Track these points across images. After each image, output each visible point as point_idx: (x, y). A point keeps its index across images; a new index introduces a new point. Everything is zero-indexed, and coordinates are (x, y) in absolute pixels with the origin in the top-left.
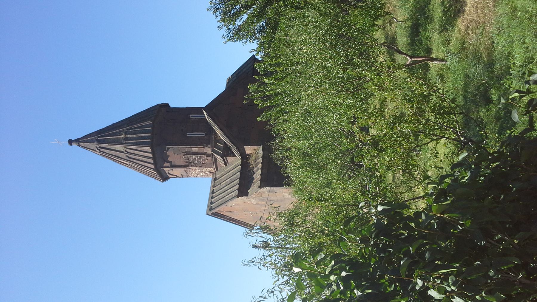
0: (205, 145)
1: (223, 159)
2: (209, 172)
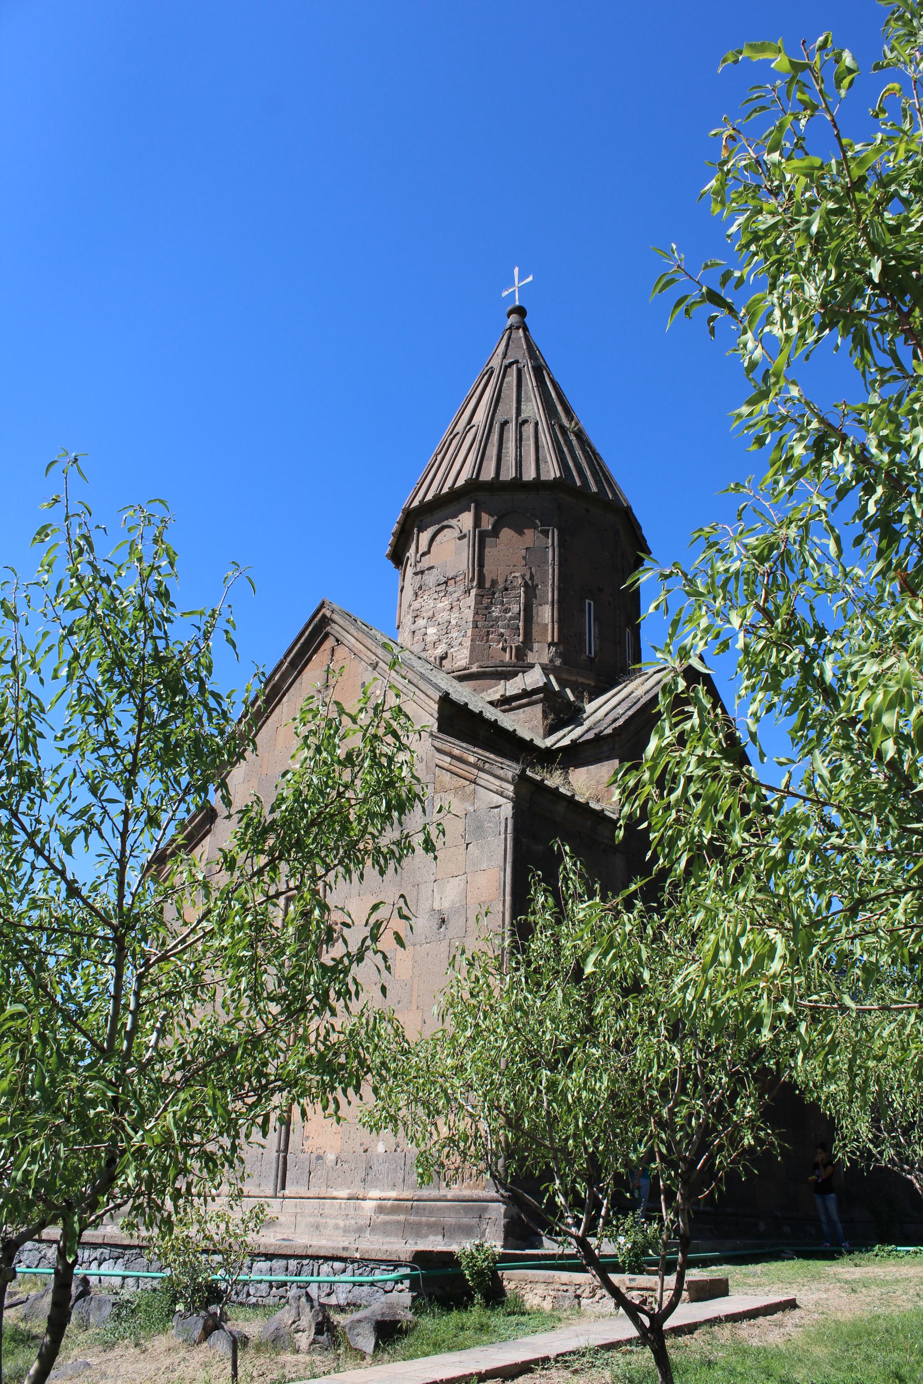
0: (561, 648)
1: (535, 691)
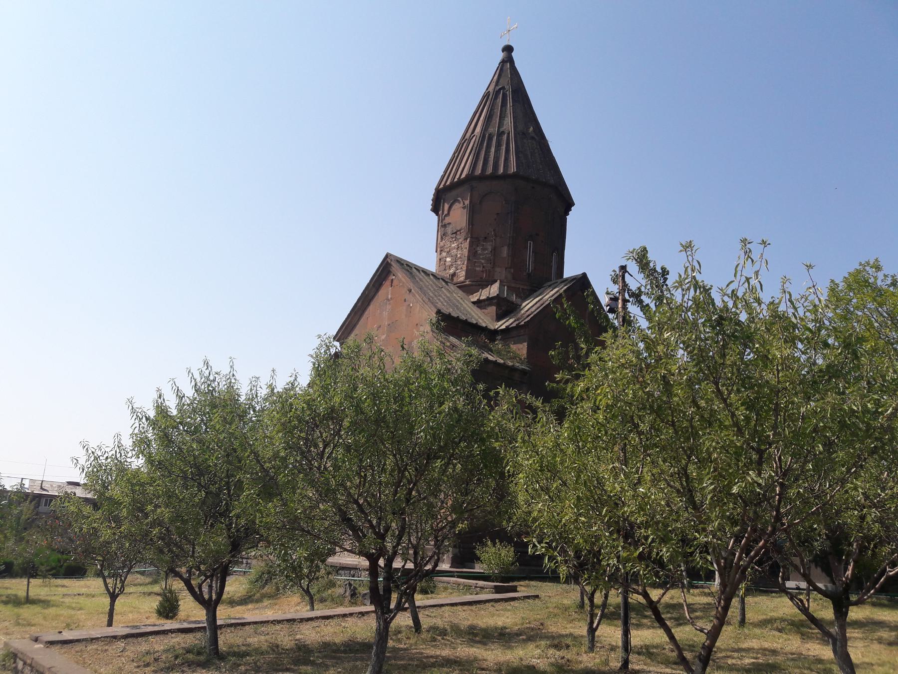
2: (455, 273)
